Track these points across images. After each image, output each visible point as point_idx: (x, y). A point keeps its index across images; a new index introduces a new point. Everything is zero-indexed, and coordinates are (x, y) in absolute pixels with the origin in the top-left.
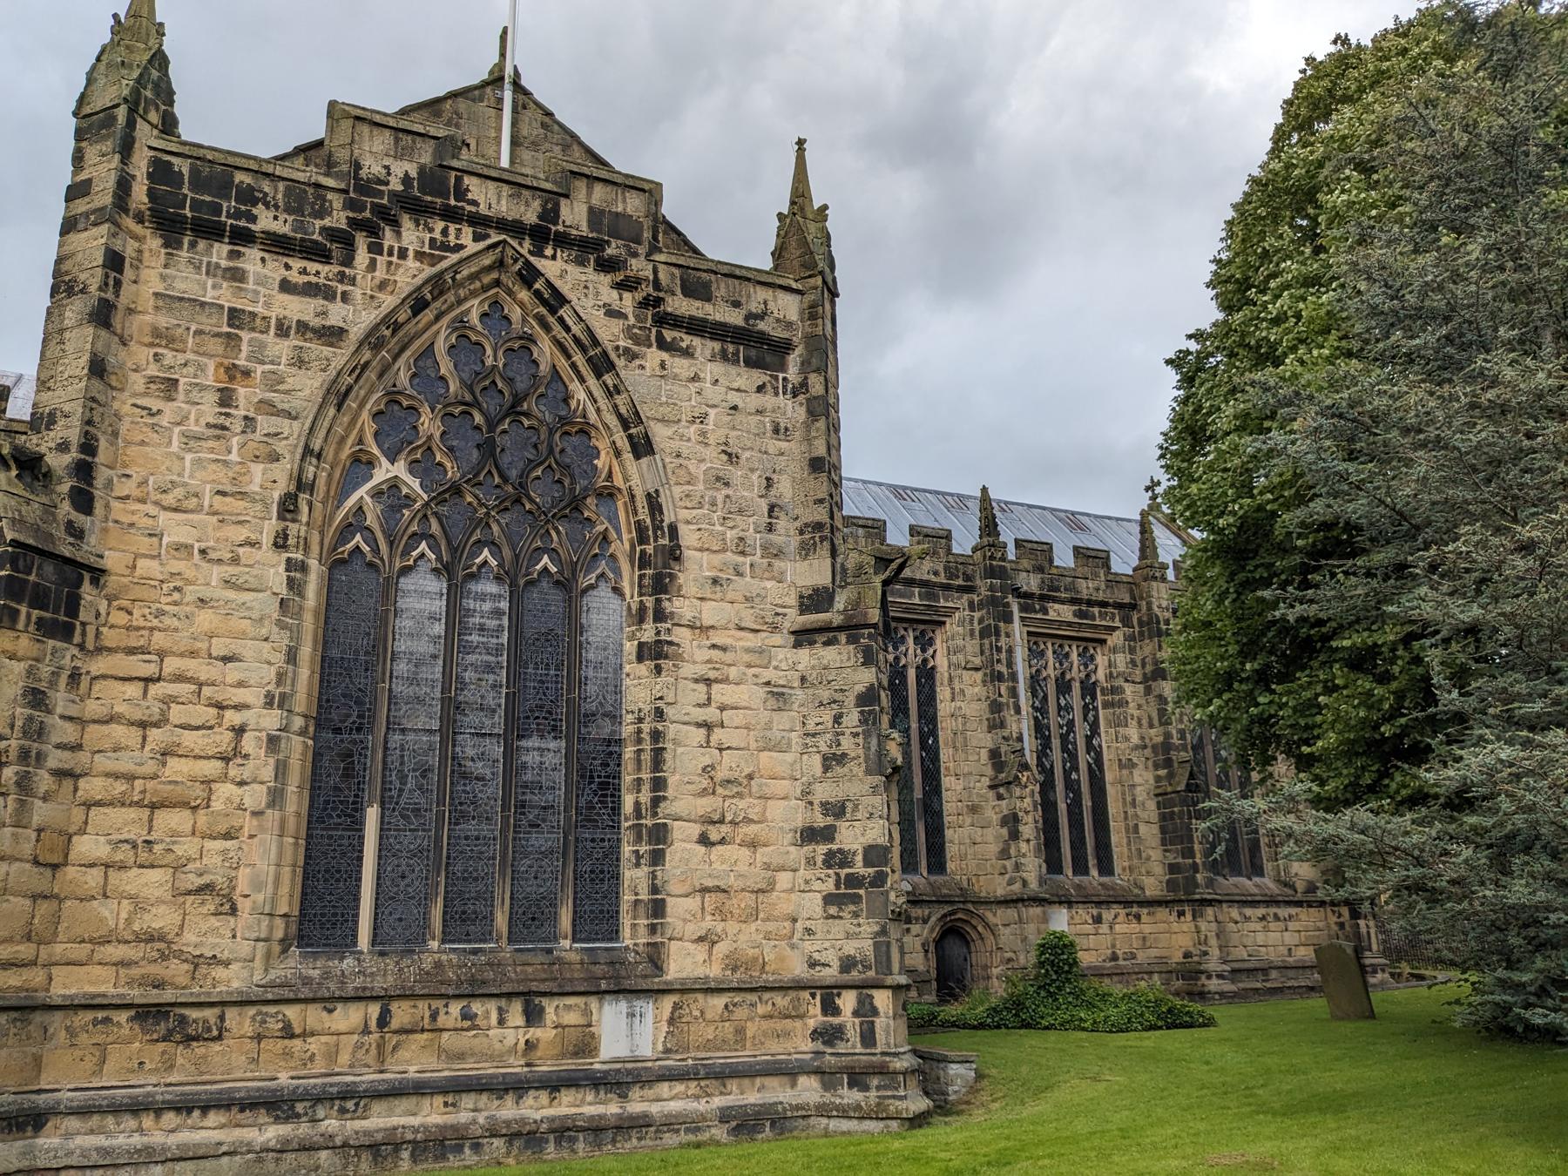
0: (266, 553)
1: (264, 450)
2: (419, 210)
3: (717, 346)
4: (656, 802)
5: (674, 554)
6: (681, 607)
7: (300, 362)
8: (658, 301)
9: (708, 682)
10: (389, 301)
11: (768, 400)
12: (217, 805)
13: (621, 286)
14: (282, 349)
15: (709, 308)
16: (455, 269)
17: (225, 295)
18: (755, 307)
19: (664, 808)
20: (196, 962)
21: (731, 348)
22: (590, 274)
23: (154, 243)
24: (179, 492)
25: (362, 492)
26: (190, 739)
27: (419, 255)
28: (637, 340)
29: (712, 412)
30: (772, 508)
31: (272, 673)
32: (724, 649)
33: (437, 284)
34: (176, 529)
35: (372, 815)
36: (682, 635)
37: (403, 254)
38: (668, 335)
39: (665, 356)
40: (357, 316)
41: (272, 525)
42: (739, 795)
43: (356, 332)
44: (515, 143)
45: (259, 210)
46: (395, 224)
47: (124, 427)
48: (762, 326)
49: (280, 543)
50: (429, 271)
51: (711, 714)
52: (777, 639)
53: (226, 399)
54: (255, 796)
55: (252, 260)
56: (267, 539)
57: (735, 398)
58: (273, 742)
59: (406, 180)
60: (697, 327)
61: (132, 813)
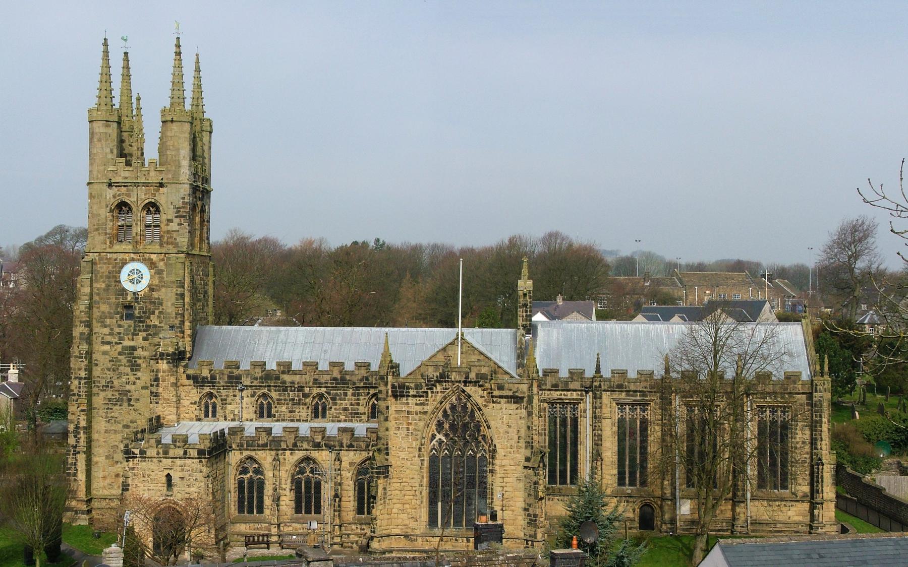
0: (417, 458)
1: (415, 439)
2: (439, 382)
3: (506, 400)
4: (492, 502)
5: (494, 451)
6: (497, 462)
7: (420, 420)
8: (492, 393)
9: (503, 478)
10: (435, 403)
11: (519, 411)
12: (413, 504)
13: (484, 390)
14: (417, 417)
15: (504, 392)
16: (448, 393)
17: (405, 408)
18: (515, 390)
19: (494, 503)
20: (412, 529)
21: (510, 400)
22: (477, 388)
23: (393, 400)
24: (401, 449)
25: (434, 442)
26: (408, 493)
27: (441, 392)
28: (487, 402)
29: (505, 416)
30: (519, 437)
31: (419, 480)
32: (506, 470)
33: (445, 398)
34: (402, 455)
35: (440, 504)
36: (497, 468)
37: (438, 392)
38: (494, 399)
39: (494, 405)
40: (429, 408)
41: (417, 454)
42: (509, 501)
43: (430, 412)
44: (462, 353)
45: (410, 390)
46: (436, 386)
47: (392, 437)
48: (517, 394)
49: (419, 456)
50: (443, 395)
51: (504, 484)
52: (520, 467)
53: (408, 429)
54: (418, 502)
55: (411, 401)
56: (417, 456)
57: (511, 412)
58: (421, 493)
59: (437, 377)
60: (501, 397)
61: (400, 505)
